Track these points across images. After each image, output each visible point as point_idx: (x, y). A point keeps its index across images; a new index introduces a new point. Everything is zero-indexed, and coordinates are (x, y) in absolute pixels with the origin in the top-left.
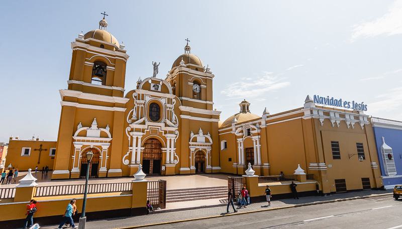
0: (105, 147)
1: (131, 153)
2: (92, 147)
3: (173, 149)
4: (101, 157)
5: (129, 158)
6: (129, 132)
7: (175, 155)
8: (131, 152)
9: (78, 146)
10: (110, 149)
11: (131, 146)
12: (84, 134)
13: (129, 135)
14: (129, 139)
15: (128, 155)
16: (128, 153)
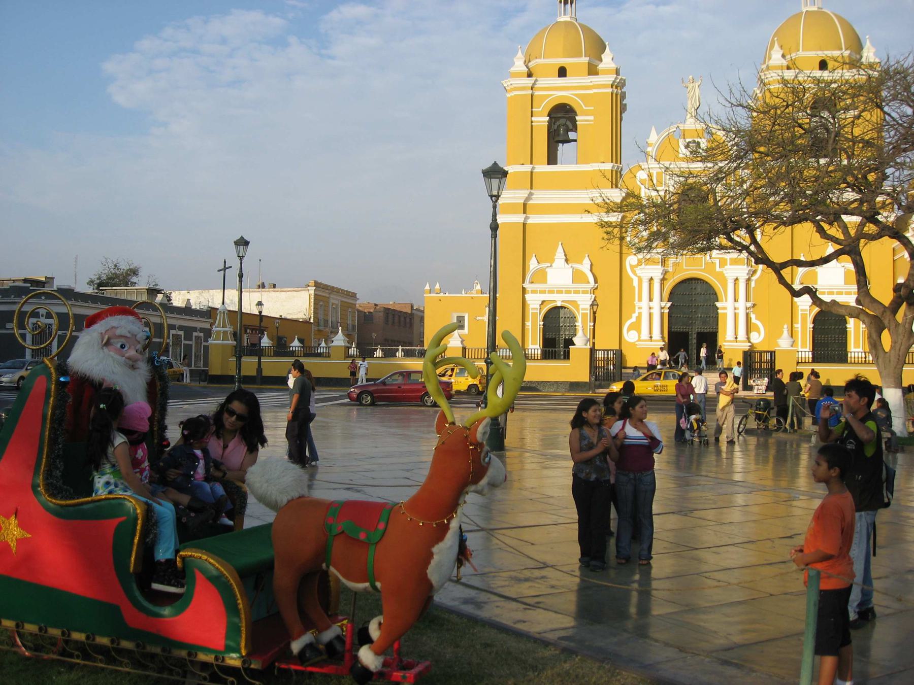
0: (584, 302)
1: (639, 318)
2: (559, 304)
3: (742, 304)
4: (579, 324)
5: (636, 326)
6: (632, 267)
7: (754, 320)
8: (640, 314)
9: (533, 301)
10: (594, 304)
11: (640, 300)
12: (541, 276)
13: (634, 273)
14: (636, 283)
15: (633, 319)
16: (635, 316)
